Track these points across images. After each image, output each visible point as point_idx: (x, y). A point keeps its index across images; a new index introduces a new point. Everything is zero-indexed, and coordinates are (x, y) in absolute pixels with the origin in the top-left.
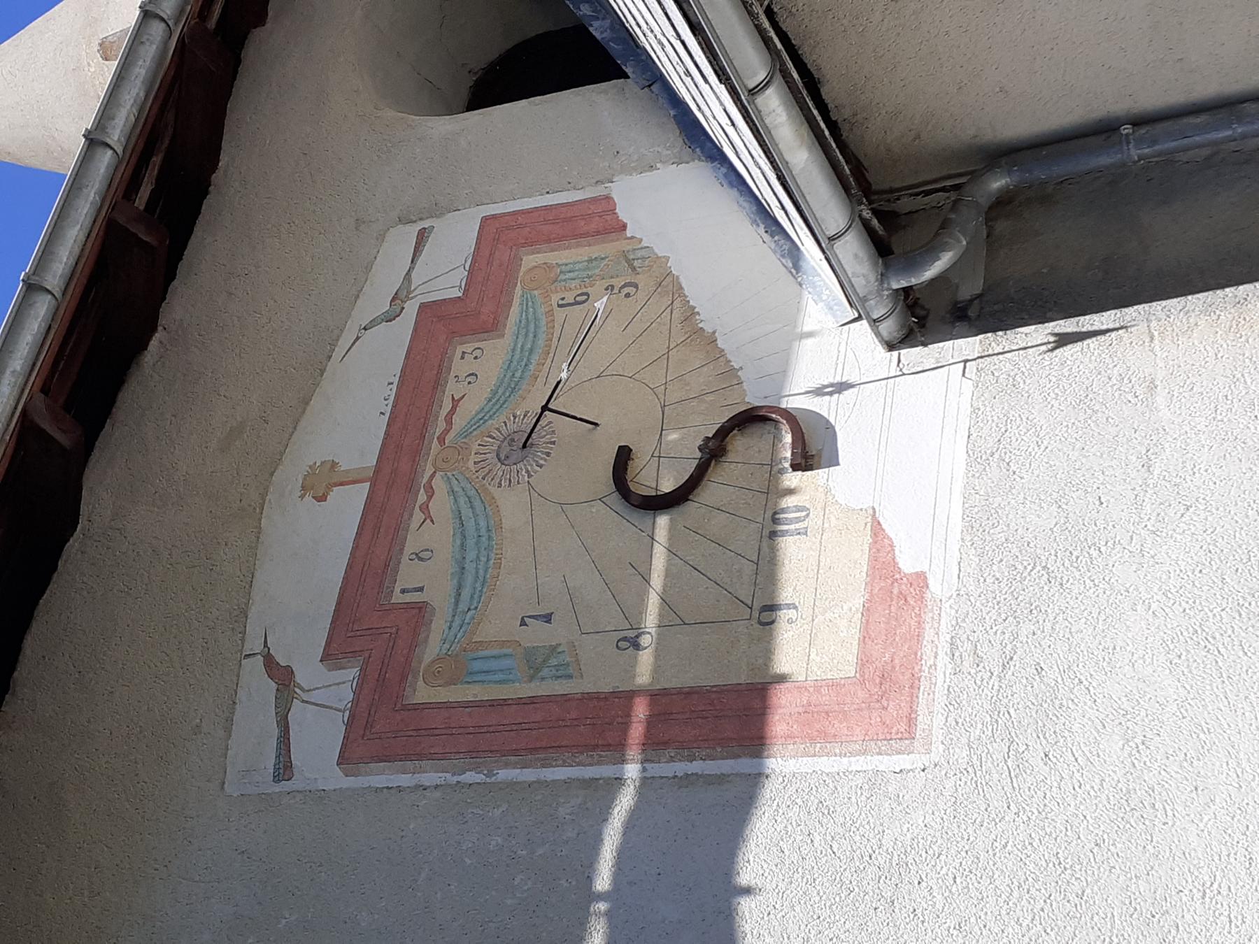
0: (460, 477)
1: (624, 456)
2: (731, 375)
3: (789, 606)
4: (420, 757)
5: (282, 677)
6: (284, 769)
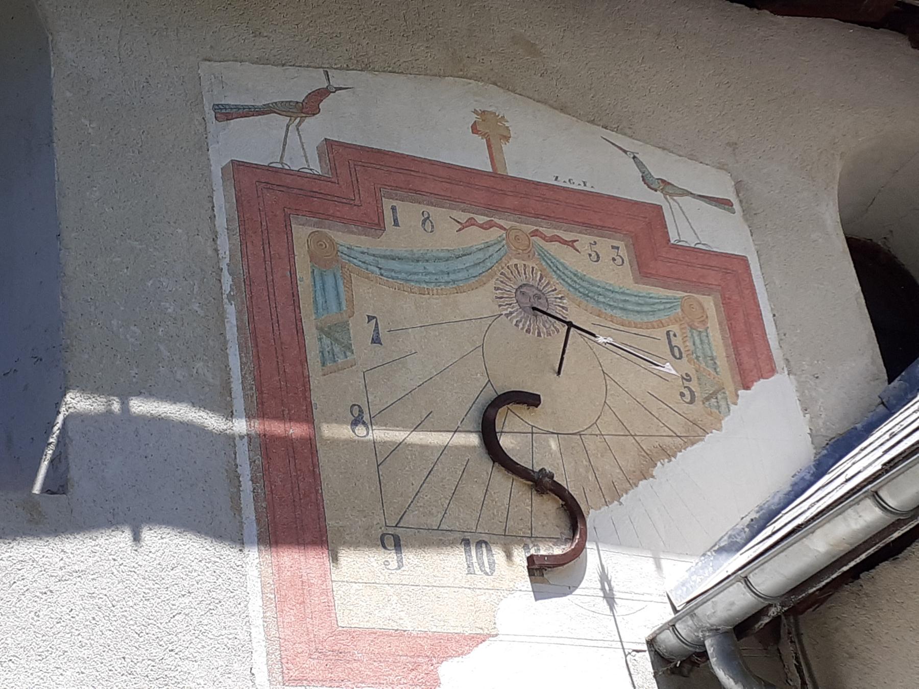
0: (502, 253)
1: (531, 400)
2: (614, 494)
3: (400, 561)
4: (243, 234)
5: (310, 106)
6: (225, 113)
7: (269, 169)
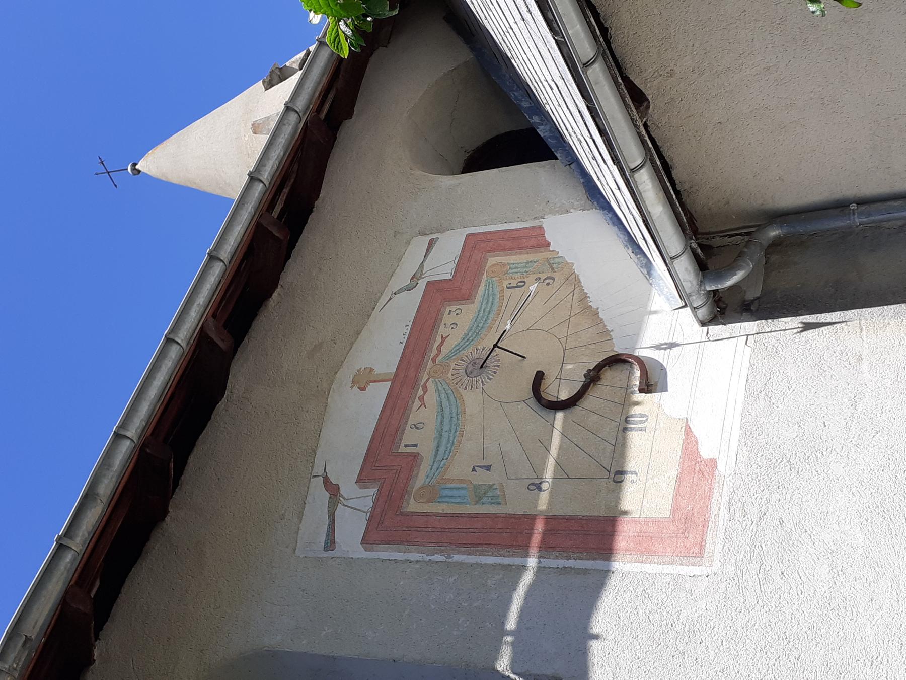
0: (443, 383)
1: (539, 377)
2: (606, 333)
3: (632, 473)
4: (408, 543)
5: (333, 490)
6: (330, 544)
7: (369, 521)
